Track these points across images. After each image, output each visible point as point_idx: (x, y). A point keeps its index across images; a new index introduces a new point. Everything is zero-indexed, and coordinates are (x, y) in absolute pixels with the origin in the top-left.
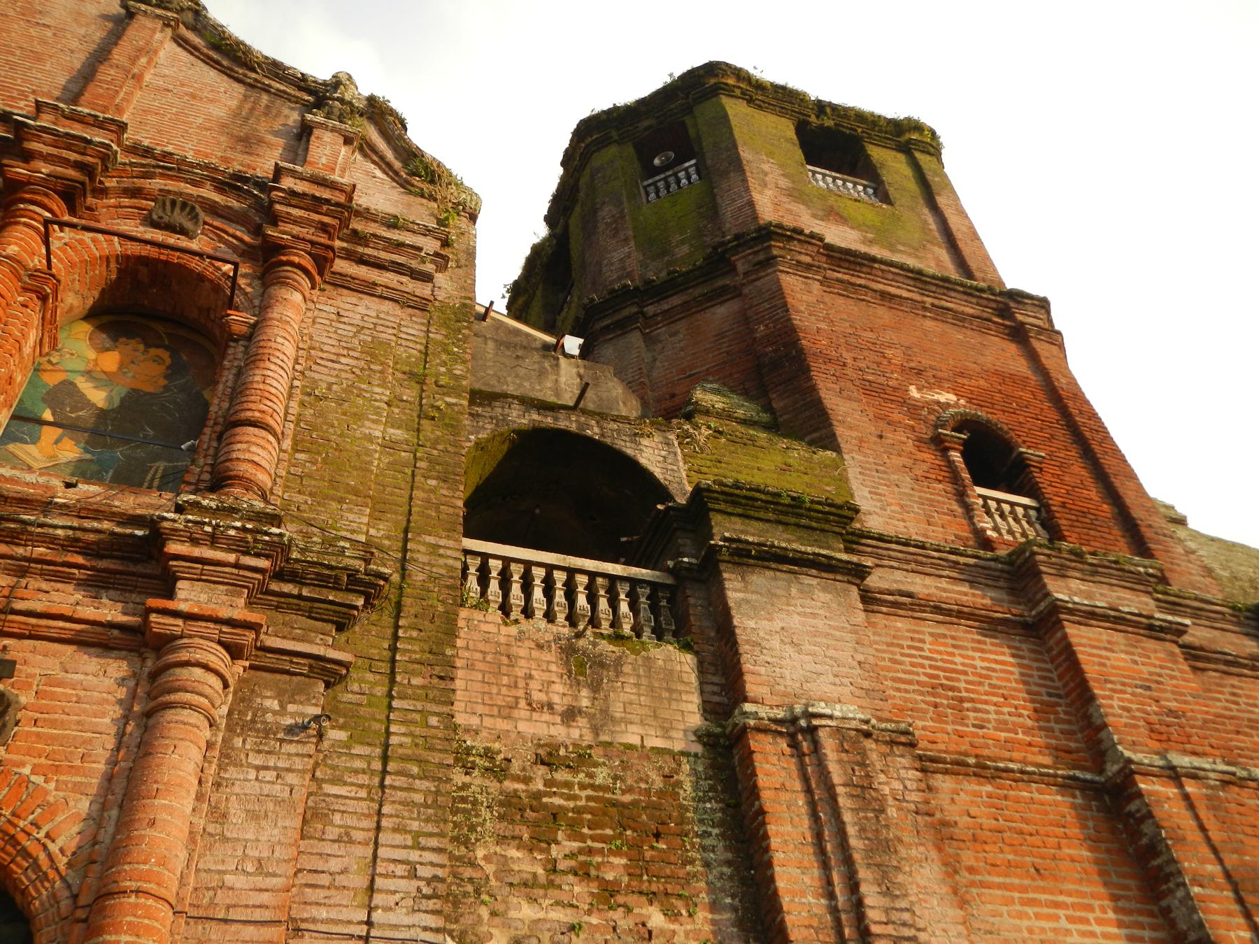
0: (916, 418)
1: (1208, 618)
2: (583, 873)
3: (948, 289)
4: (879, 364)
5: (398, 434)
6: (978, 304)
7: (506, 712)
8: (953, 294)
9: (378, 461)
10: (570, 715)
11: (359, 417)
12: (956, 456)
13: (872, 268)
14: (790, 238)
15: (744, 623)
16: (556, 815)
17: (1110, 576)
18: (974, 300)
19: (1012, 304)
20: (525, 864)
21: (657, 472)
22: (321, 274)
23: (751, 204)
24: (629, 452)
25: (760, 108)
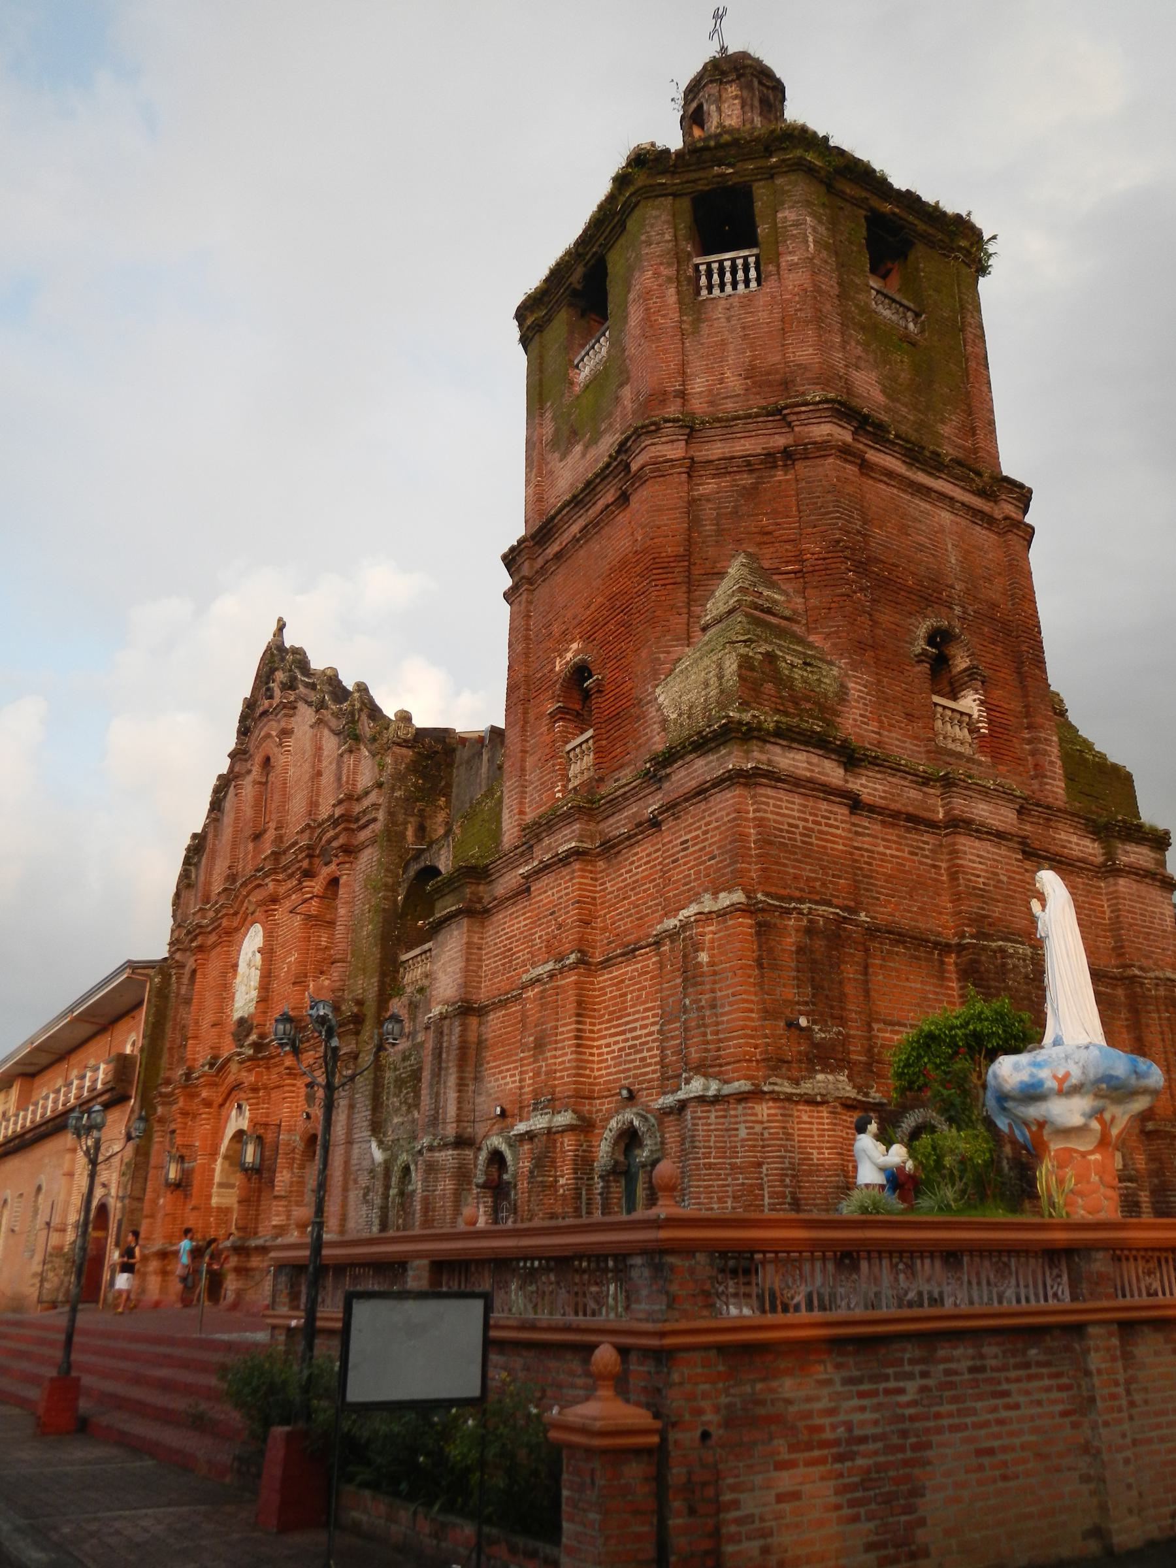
1: (633, 796)
2: (405, 1102)
3: (593, 489)
6: (615, 478)
8: (599, 489)
11: (362, 926)
13: (555, 525)
17: (557, 823)
18: (610, 479)
19: (625, 458)
22: (351, 852)
25: (550, 320)
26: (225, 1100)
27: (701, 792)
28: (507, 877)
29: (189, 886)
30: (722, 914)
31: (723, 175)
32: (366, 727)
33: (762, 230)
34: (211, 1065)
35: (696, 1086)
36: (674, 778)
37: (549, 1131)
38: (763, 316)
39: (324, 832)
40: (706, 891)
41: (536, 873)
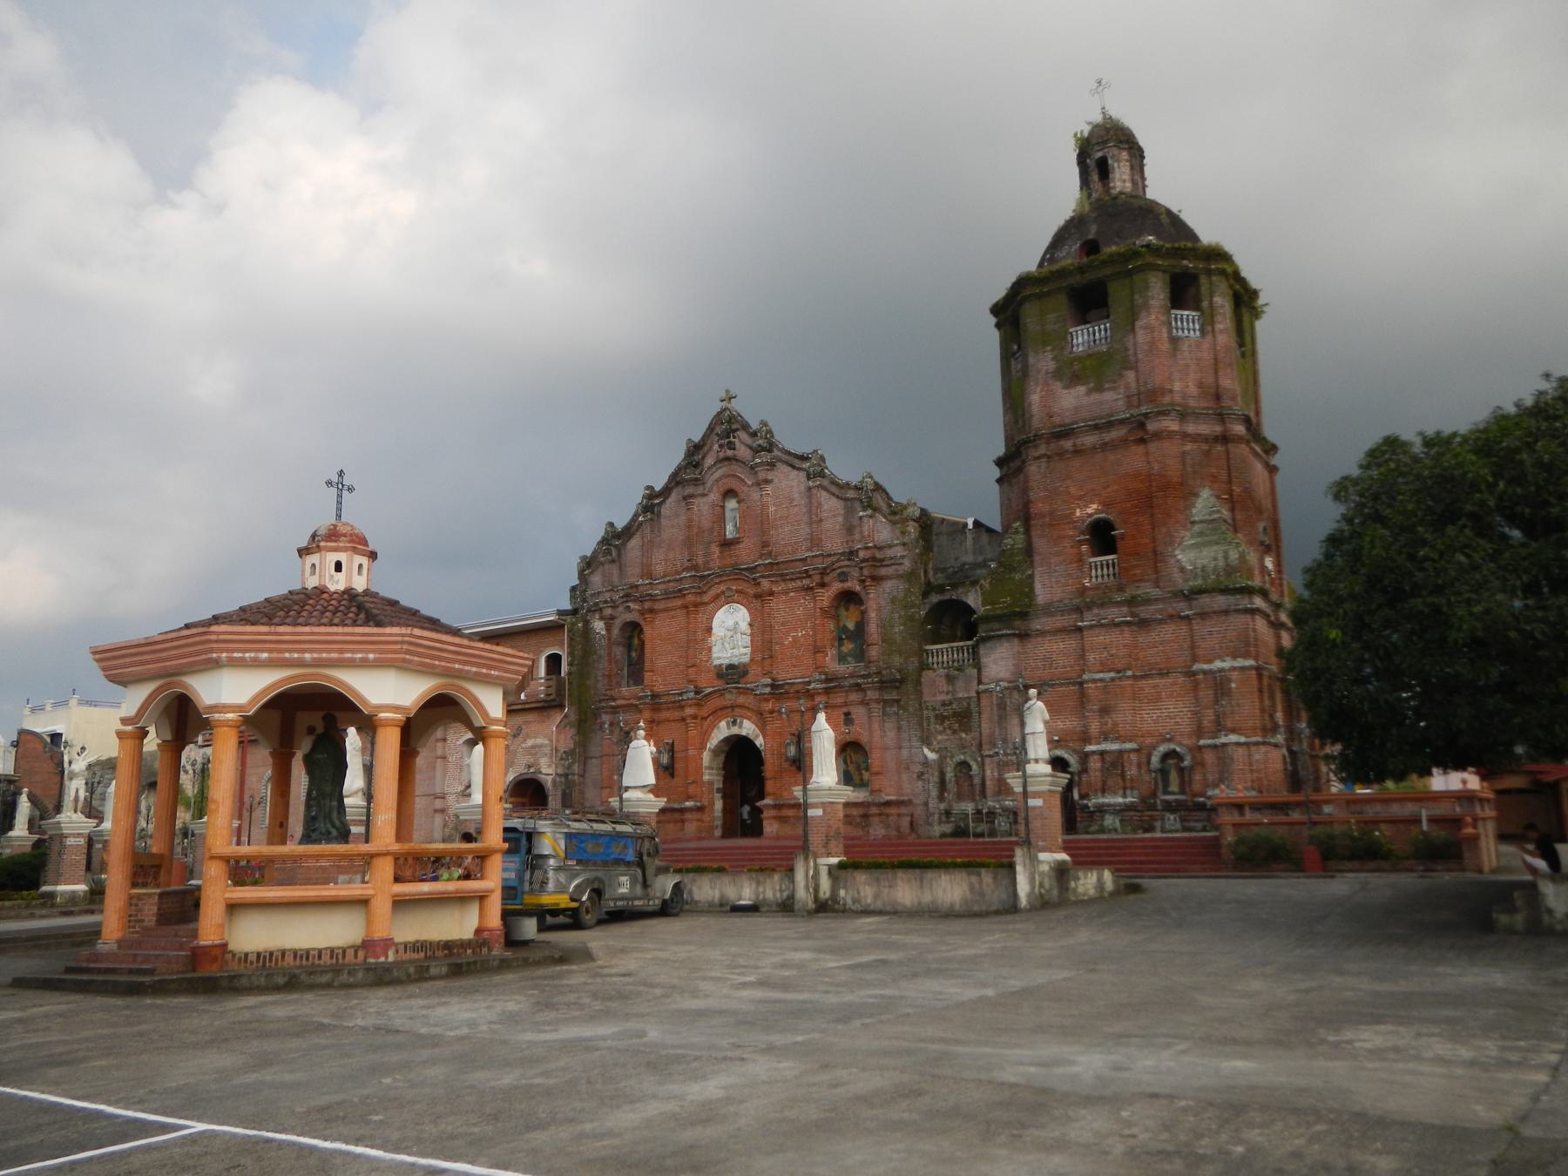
0: (1075, 528)
2: (950, 728)
4: (1065, 501)
5: (902, 627)
7: (935, 695)
9: (898, 638)
10: (948, 693)
11: (893, 626)
12: (1084, 548)
14: (1034, 440)
15: (984, 660)
16: (946, 717)
20: (940, 728)
21: (972, 605)
23: (1030, 405)
24: (964, 600)
26: (708, 716)
27: (1226, 612)
28: (1044, 620)
29: (613, 561)
30: (1242, 669)
31: (1187, 267)
32: (879, 500)
33: (1205, 304)
34: (697, 693)
35: (1233, 738)
36: (1201, 600)
37: (1121, 752)
38: (1206, 354)
39: (838, 561)
40: (1227, 655)
41: (1091, 627)
